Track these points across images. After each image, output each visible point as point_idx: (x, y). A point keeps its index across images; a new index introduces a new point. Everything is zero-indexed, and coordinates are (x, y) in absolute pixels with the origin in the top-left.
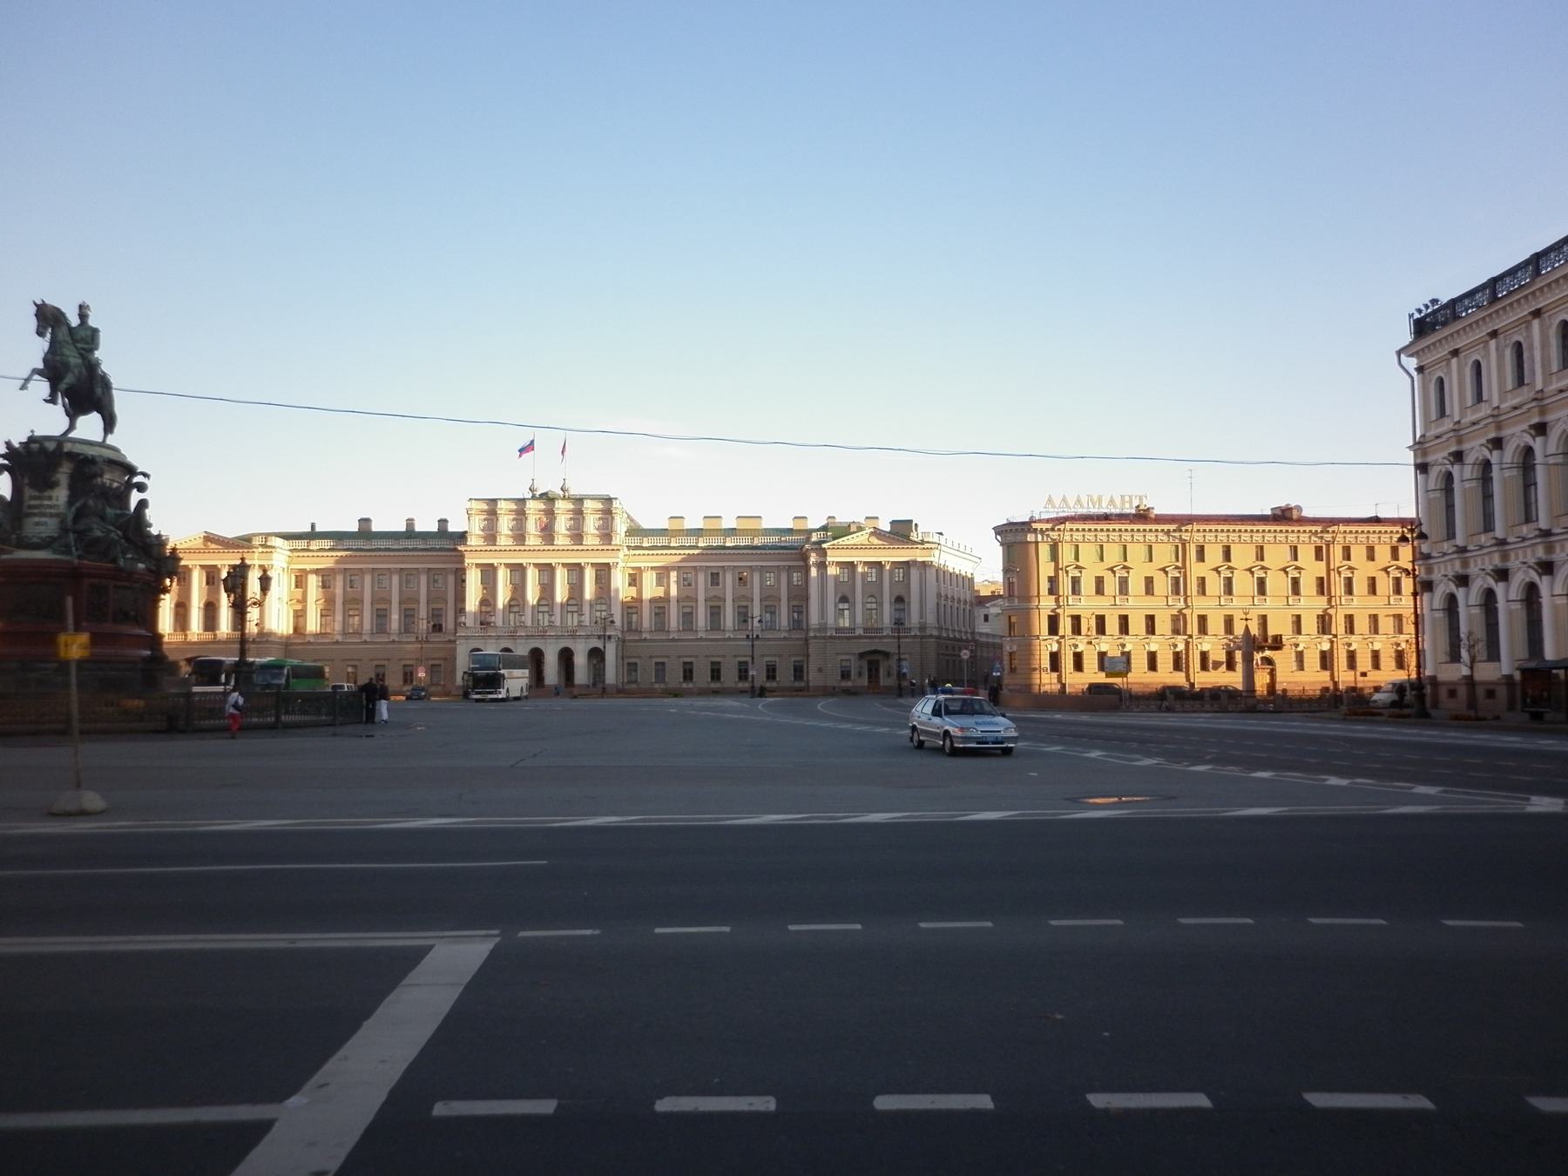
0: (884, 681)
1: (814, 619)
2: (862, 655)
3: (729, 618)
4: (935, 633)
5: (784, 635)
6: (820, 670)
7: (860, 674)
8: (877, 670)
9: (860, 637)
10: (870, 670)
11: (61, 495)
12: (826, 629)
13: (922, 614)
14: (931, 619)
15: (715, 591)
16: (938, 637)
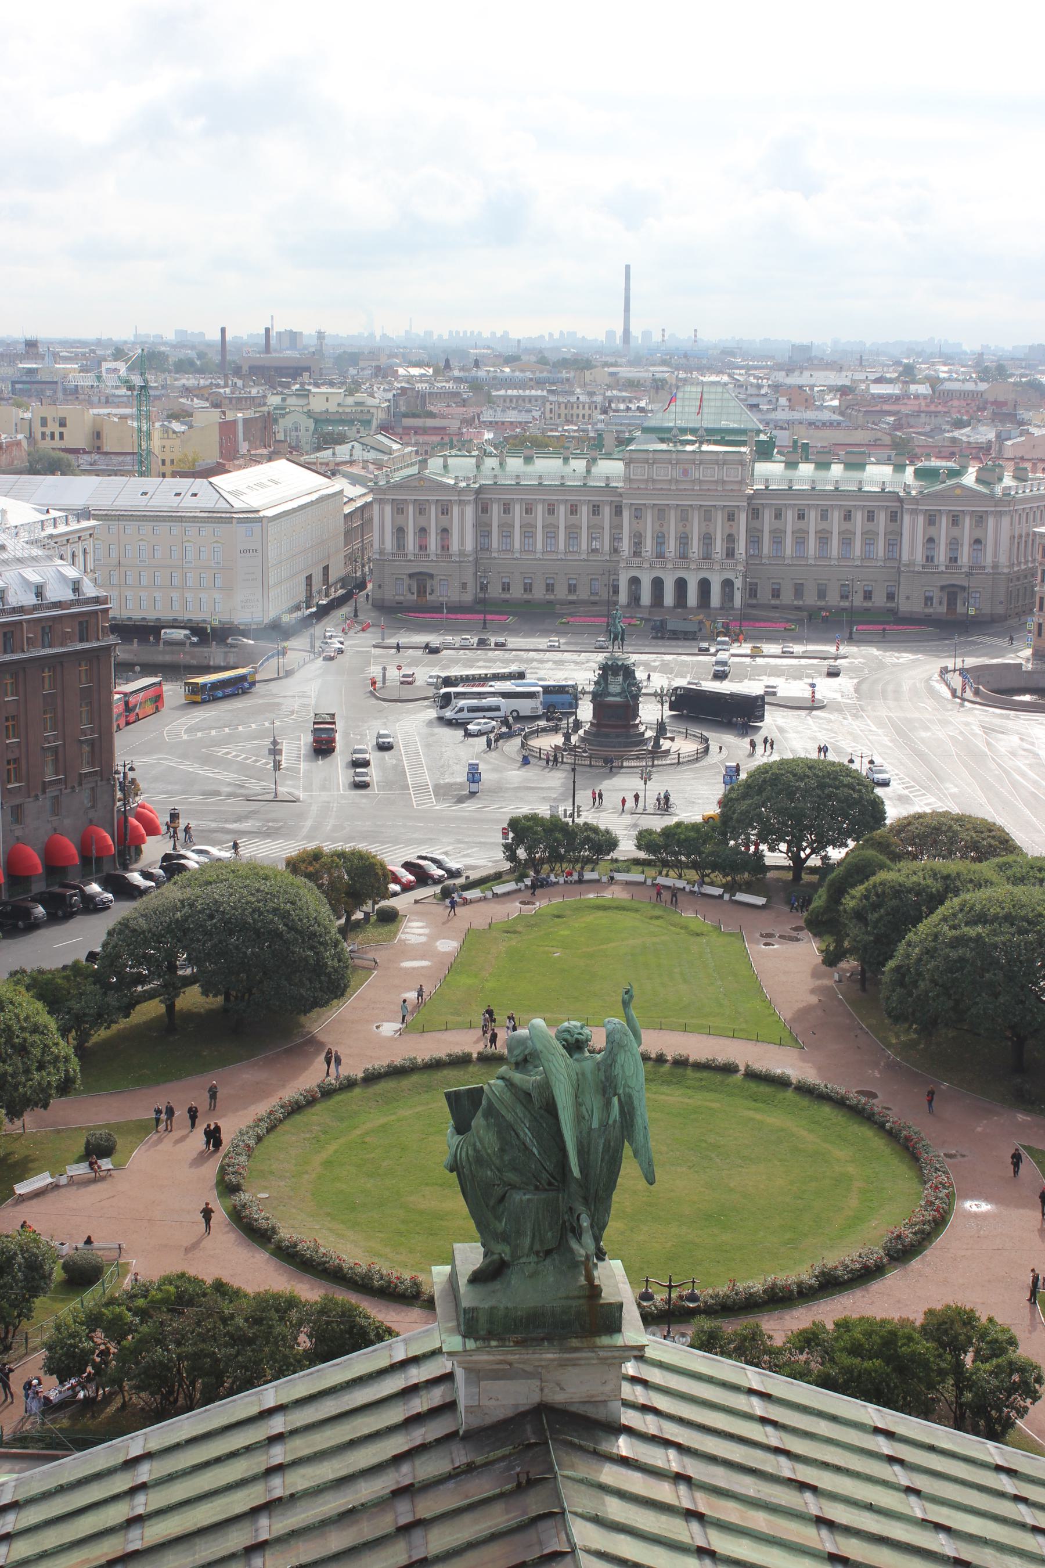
0: (960, 609)
1: (905, 557)
2: (942, 588)
3: (835, 547)
4: (1006, 570)
5: (881, 563)
6: (908, 598)
7: (940, 603)
8: (956, 599)
9: (942, 572)
10: (949, 599)
11: (621, 678)
12: (914, 565)
13: (995, 554)
14: (1003, 559)
15: (824, 525)
16: (1009, 573)
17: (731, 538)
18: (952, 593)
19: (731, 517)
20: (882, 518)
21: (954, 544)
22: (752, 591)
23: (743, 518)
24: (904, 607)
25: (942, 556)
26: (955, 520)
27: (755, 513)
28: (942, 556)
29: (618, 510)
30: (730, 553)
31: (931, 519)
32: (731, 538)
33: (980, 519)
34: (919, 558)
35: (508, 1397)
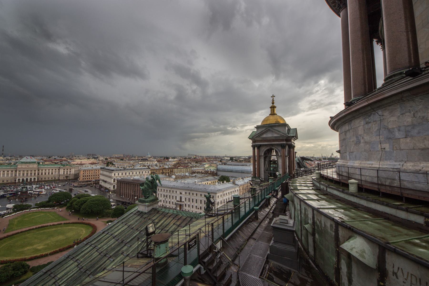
17: (35, 173)
18: (67, 177)
19: (35, 171)
20: (57, 170)
21: (67, 172)
22: (38, 179)
23: (37, 171)
24: (60, 179)
25: (66, 173)
26: (67, 169)
27: (38, 170)
28: (66, 173)
29: (16, 171)
30: (35, 175)
31: (64, 170)
32: (35, 173)
33: (70, 169)
34: (63, 173)
35: (150, 208)
